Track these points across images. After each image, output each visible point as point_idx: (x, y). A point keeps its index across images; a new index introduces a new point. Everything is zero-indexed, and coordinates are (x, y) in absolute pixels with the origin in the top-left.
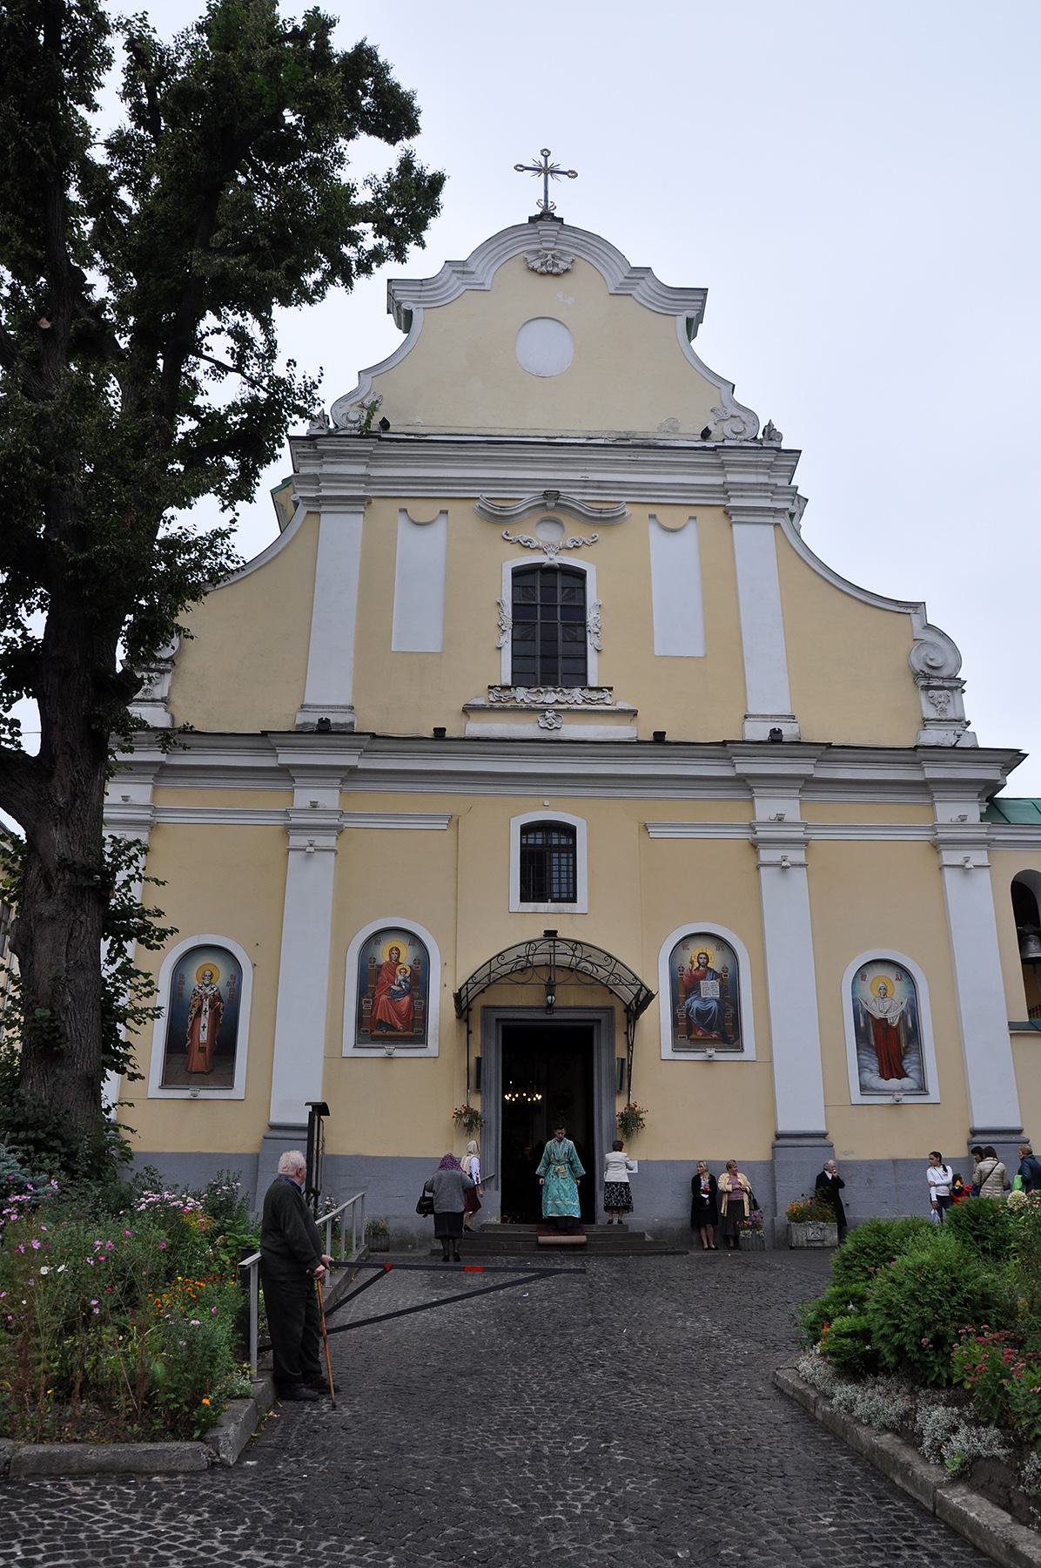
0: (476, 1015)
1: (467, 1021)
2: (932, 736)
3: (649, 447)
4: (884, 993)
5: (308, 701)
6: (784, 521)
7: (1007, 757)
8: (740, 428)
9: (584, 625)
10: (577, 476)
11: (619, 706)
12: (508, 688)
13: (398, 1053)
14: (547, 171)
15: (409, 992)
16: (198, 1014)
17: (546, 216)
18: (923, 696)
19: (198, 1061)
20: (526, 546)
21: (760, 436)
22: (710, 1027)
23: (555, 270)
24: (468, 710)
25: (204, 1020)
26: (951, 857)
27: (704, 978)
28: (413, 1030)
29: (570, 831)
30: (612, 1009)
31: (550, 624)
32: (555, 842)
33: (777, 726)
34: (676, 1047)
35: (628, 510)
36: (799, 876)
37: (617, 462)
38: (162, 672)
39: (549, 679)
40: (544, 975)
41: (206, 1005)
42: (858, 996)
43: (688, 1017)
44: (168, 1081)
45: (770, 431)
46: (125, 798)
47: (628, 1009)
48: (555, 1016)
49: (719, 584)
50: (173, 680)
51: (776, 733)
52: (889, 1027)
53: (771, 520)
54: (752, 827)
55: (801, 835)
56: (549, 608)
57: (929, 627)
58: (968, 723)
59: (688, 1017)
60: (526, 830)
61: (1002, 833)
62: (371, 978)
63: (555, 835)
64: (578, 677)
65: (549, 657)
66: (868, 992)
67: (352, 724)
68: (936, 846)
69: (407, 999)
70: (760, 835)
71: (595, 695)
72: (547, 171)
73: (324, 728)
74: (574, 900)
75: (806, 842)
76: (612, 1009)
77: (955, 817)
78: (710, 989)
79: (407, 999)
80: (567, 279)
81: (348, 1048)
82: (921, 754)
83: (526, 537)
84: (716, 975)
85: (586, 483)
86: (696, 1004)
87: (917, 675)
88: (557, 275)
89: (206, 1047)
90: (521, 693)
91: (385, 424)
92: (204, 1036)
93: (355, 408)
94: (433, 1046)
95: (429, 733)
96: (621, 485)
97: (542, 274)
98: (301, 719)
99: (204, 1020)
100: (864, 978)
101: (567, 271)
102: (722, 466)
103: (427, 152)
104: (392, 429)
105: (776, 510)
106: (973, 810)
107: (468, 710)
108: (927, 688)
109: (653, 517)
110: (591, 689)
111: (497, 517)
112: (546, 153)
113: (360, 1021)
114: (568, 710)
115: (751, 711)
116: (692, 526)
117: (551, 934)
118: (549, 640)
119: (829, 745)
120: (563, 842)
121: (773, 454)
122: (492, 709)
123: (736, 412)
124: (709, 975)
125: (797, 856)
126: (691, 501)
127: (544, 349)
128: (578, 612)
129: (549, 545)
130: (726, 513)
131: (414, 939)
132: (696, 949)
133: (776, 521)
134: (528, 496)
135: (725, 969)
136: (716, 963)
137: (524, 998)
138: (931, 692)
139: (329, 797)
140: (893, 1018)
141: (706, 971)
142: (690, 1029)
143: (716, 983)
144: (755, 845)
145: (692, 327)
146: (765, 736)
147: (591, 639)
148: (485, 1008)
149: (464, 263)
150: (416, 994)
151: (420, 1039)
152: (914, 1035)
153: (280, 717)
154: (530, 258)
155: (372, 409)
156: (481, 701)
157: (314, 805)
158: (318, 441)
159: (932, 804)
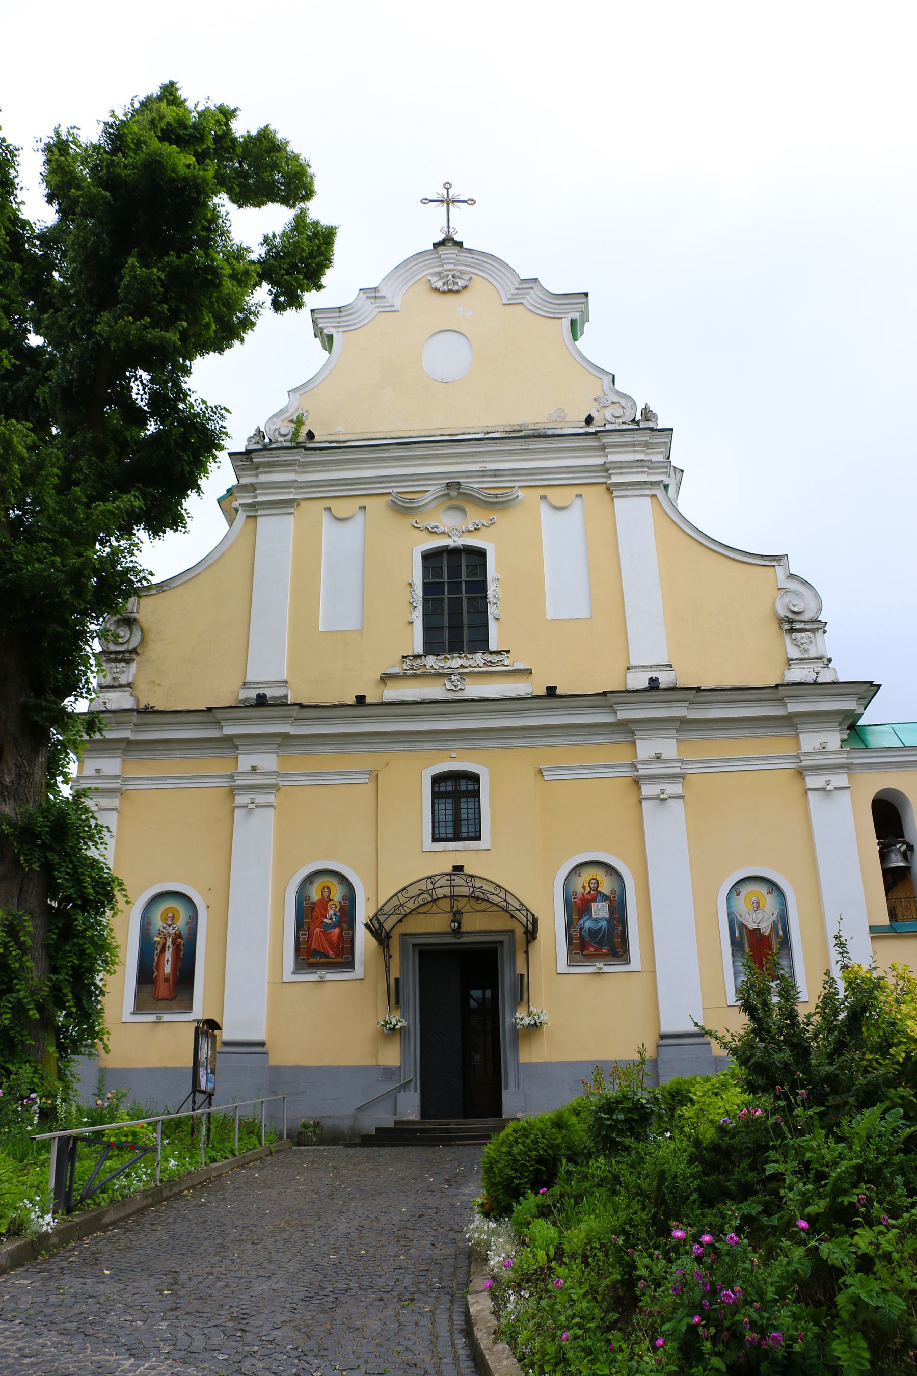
0: (395, 943)
1: (388, 947)
2: (798, 674)
3: (540, 436)
4: (757, 906)
5: (249, 679)
6: (659, 493)
7: (862, 689)
8: (619, 412)
9: (486, 597)
10: (477, 467)
11: (516, 667)
12: (418, 657)
13: (329, 977)
14: (448, 201)
15: (339, 924)
16: (163, 950)
17: (448, 242)
18: (787, 639)
19: (163, 989)
20: (432, 532)
21: (639, 417)
22: (600, 944)
23: (456, 288)
24: (386, 678)
25: (168, 955)
26: (813, 781)
27: (594, 900)
28: (341, 956)
29: (475, 778)
30: (513, 931)
31: (455, 598)
32: (463, 788)
33: (654, 675)
34: (571, 962)
35: (521, 493)
36: (677, 806)
37: (510, 452)
38: (128, 662)
39: (456, 647)
40: (445, 905)
41: (169, 942)
42: (733, 909)
43: (582, 937)
44: (139, 1007)
45: (647, 414)
46: (98, 771)
47: (526, 932)
48: (465, 939)
49: (604, 554)
50: (138, 669)
51: (653, 681)
52: (762, 936)
53: (647, 492)
54: (634, 766)
55: (678, 770)
56: (455, 587)
57: (792, 576)
58: (830, 660)
59: (582, 937)
60: (437, 780)
61: (860, 759)
62: (307, 914)
63: (463, 782)
64: (481, 643)
65: (456, 627)
66: (742, 905)
67: (286, 696)
68: (801, 773)
69: (337, 930)
70: (641, 772)
71: (494, 658)
72: (448, 201)
73: (261, 701)
74: (479, 838)
75: (682, 776)
76: (513, 931)
77: (817, 745)
78: (600, 910)
79: (337, 930)
80: (465, 295)
81: (288, 975)
82: (782, 692)
83: (433, 524)
84: (605, 898)
85: (483, 473)
86: (588, 924)
87: (782, 620)
88: (457, 292)
89: (169, 977)
90: (431, 661)
91: (310, 435)
92: (168, 969)
93: (286, 423)
94: (359, 970)
95: (351, 700)
96: (515, 472)
97: (444, 292)
98: (243, 694)
99: (168, 955)
100: (738, 893)
101: (465, 287)
102: (603, 448)
103: (318, 210)
104: (317, 439)
105: (651, 483)
106: (833, 739)
107: (386, 678)
108: (792, 631)
109: (544, 498)
110: (492, 653)
111: (404, 508)
112: (448, 186)
113: (298, 950)
114: (471, 673)
115: (633, 663)
116: (578, 502)
117: (458, 869)
118: (455, 613)
119: (699, 689)
120: (471, 788)
121: (648, 430)
122: (404, 676)
123: (616, 399)
124: (599, 898)
125: (674, 788)
126: (575, 479)
127: (446, 358)
128: (480, 586)
129: (453, 530)
130: (608, 489)
131: (343, 879)
132: (587, 875)
133: (653, 492)
134: (434, 489)
135: (613, 892)
136: (606, 886)
137: (435, 924)
138: (795, 635)
139: (268, 761)
141: (596, 895)
142: (583, 946)
143: (605, 905)
144: (637, 782)
145: (575, 328)
146: (644, 684)
147: (491, 610)
148: (404, 935)
149: (376, 289)
150: (345, 926)
151: (349, 964)
152: (786, 942)
153: (223, 692)
154: (433, 279)
155: (299, 422)
156: (397, 670)
157: (254, 768)
158: (253, 455)
159: (797, 736)
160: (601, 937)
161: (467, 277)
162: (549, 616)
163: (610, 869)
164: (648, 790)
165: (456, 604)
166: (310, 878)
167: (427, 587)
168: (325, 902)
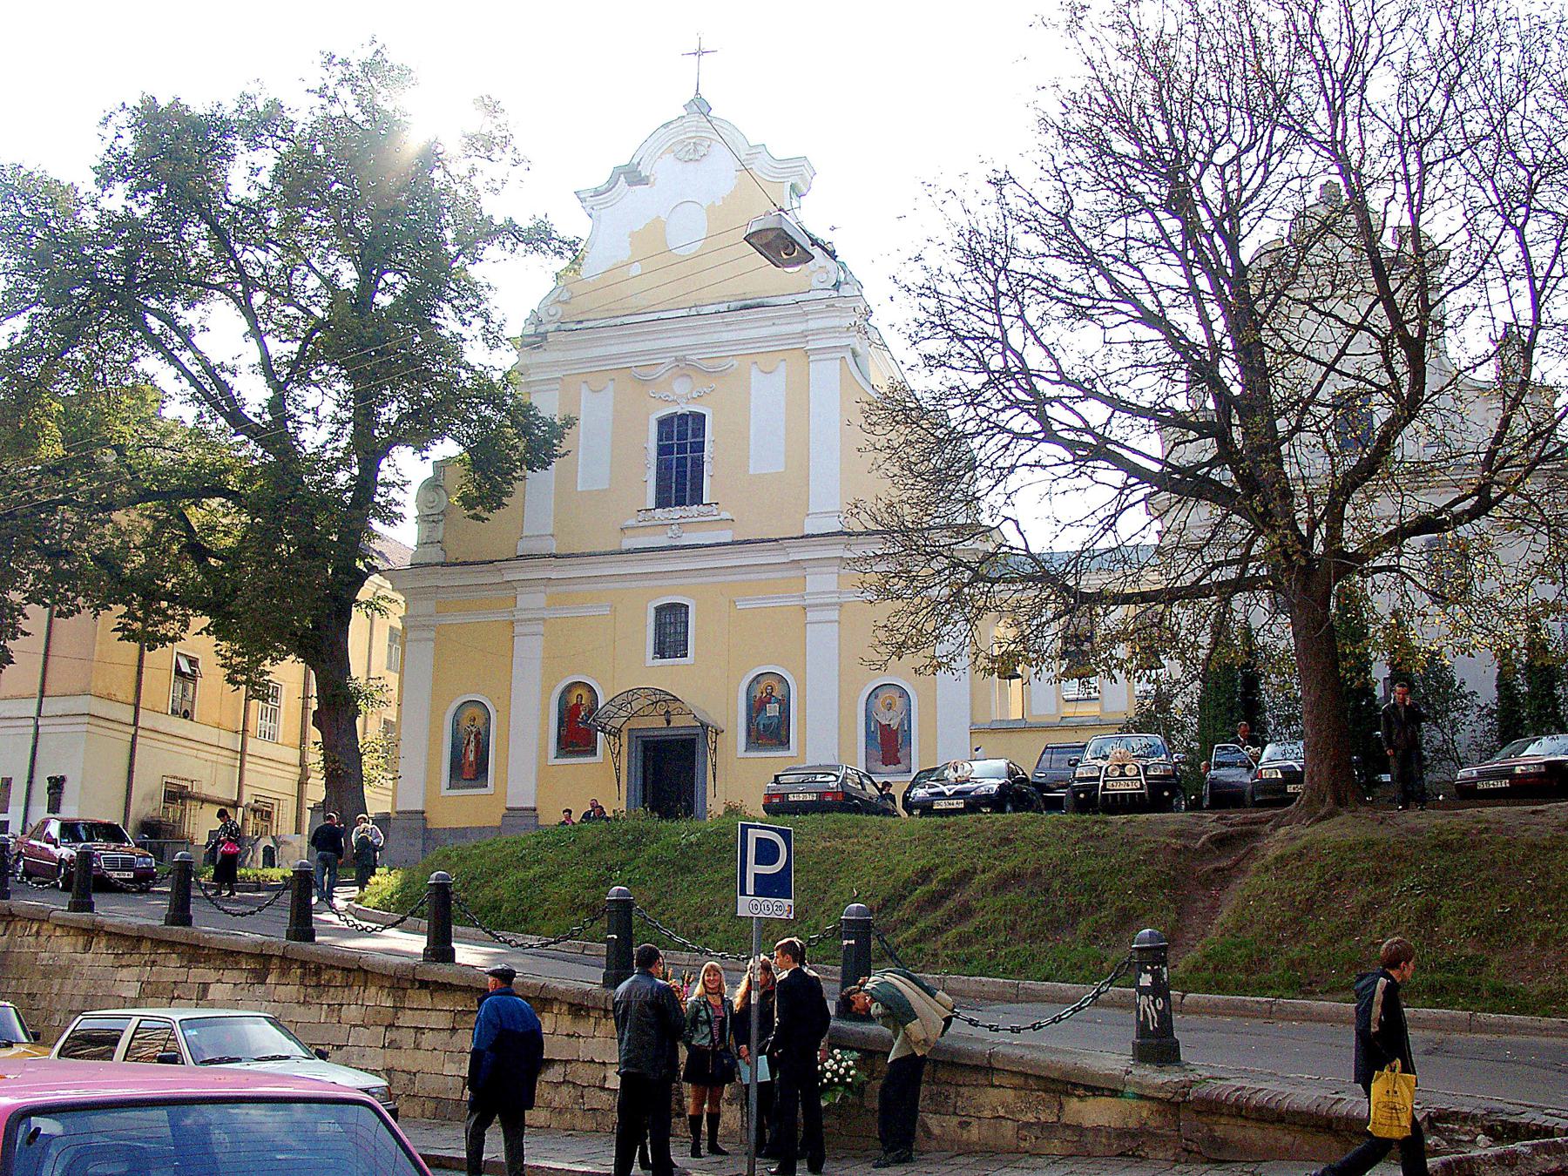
6: (849, 356)
19: (469, 772)
39: (680, 502)
64: (697, 499)
81: (552, 761)
92: (472, 758)
99: (472, 747)
125: (834, 615)
128: (700, 447)
140: (894, 724)
160: (769, 729)
161: (706, 144)
162: (751, 472)
163: (782, 679)
164: (811, 616)
165: (681, 463)
166: (569, 689)
167: (663, 450)
168: (577, 706)
